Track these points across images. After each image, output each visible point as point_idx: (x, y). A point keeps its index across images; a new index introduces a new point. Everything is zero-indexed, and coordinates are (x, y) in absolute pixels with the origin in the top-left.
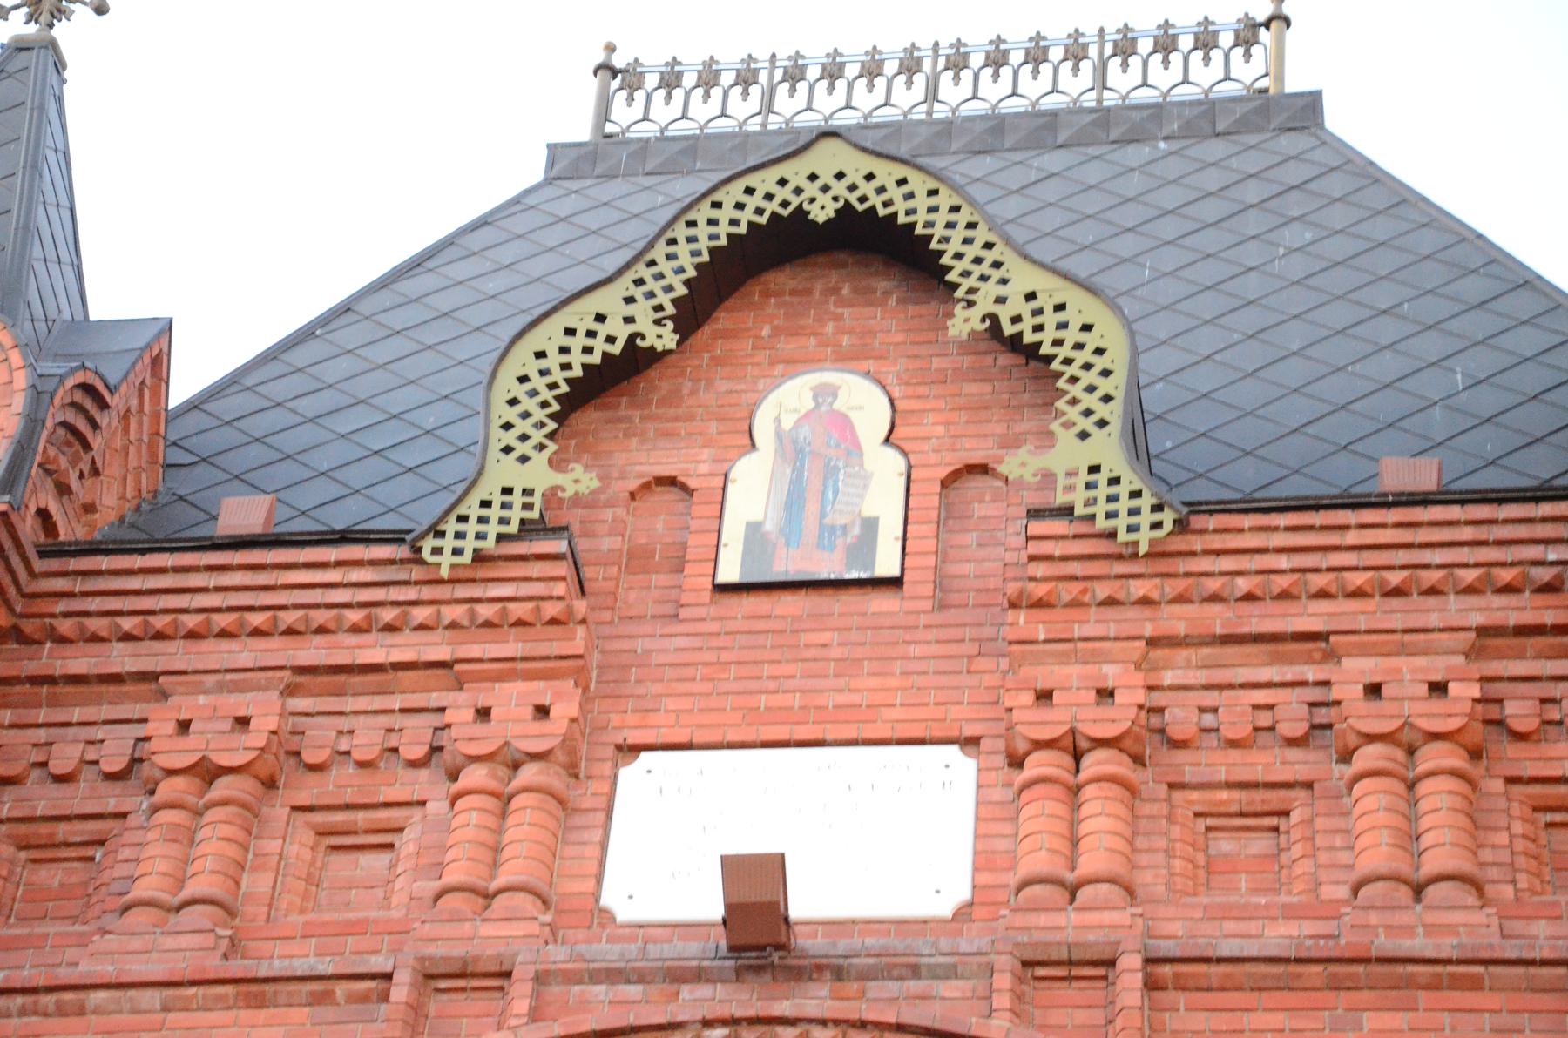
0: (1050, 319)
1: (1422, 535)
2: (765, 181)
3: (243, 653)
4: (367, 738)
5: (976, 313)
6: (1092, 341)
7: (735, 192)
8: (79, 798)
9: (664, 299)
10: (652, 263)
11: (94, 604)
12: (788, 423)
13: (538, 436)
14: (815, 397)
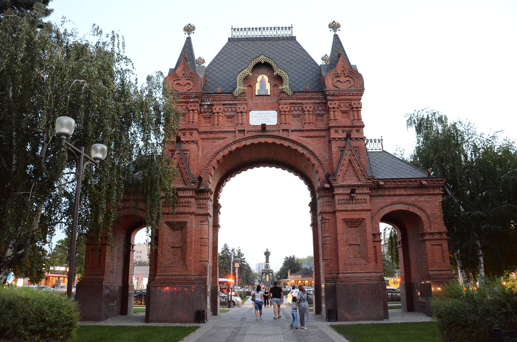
0: (282, 74)
2: (258, 59)
6: (285, 76)
7: (255, 60)
13: (242, 84)
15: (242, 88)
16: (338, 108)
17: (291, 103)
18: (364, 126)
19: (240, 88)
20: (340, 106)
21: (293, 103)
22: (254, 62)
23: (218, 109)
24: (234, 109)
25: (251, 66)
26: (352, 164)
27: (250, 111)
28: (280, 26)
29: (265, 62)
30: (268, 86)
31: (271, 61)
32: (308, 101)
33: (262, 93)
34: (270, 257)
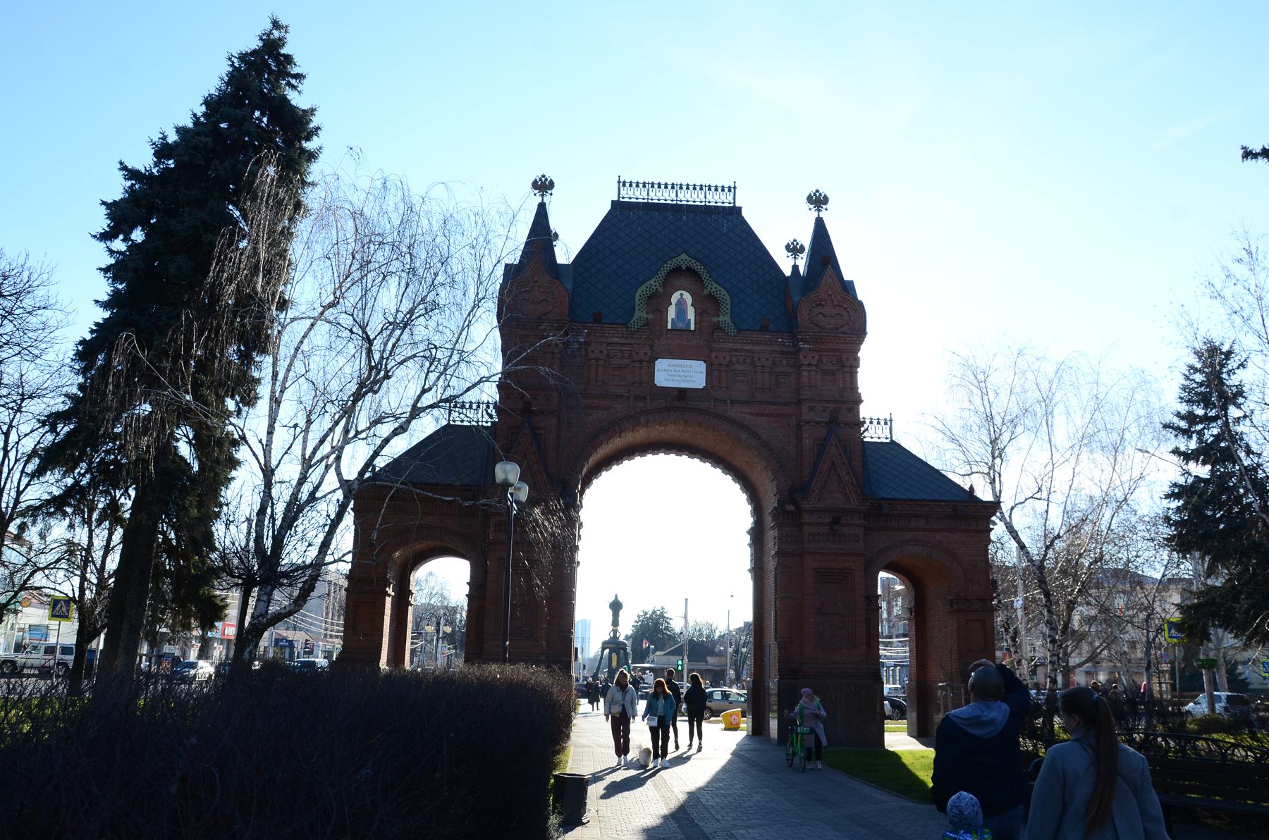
2: (675, 260)
15: (644, 315)
16: (817, 366)
17: (731, 350)
18: (862, 401)
19: (640, 314)
20: (820, 361)
21: (736, 350)
22: (669, 266)
23: (597, 351)
24: (627, 355)
25: (662, 274)
26: (836, 470)
27: (657, 359)
28: (713, 184)
29: (687, 267)
30: (691, 314)
31: (699, 267)
32: (762, 348)
33: (680, 325)
34: (621, 613)
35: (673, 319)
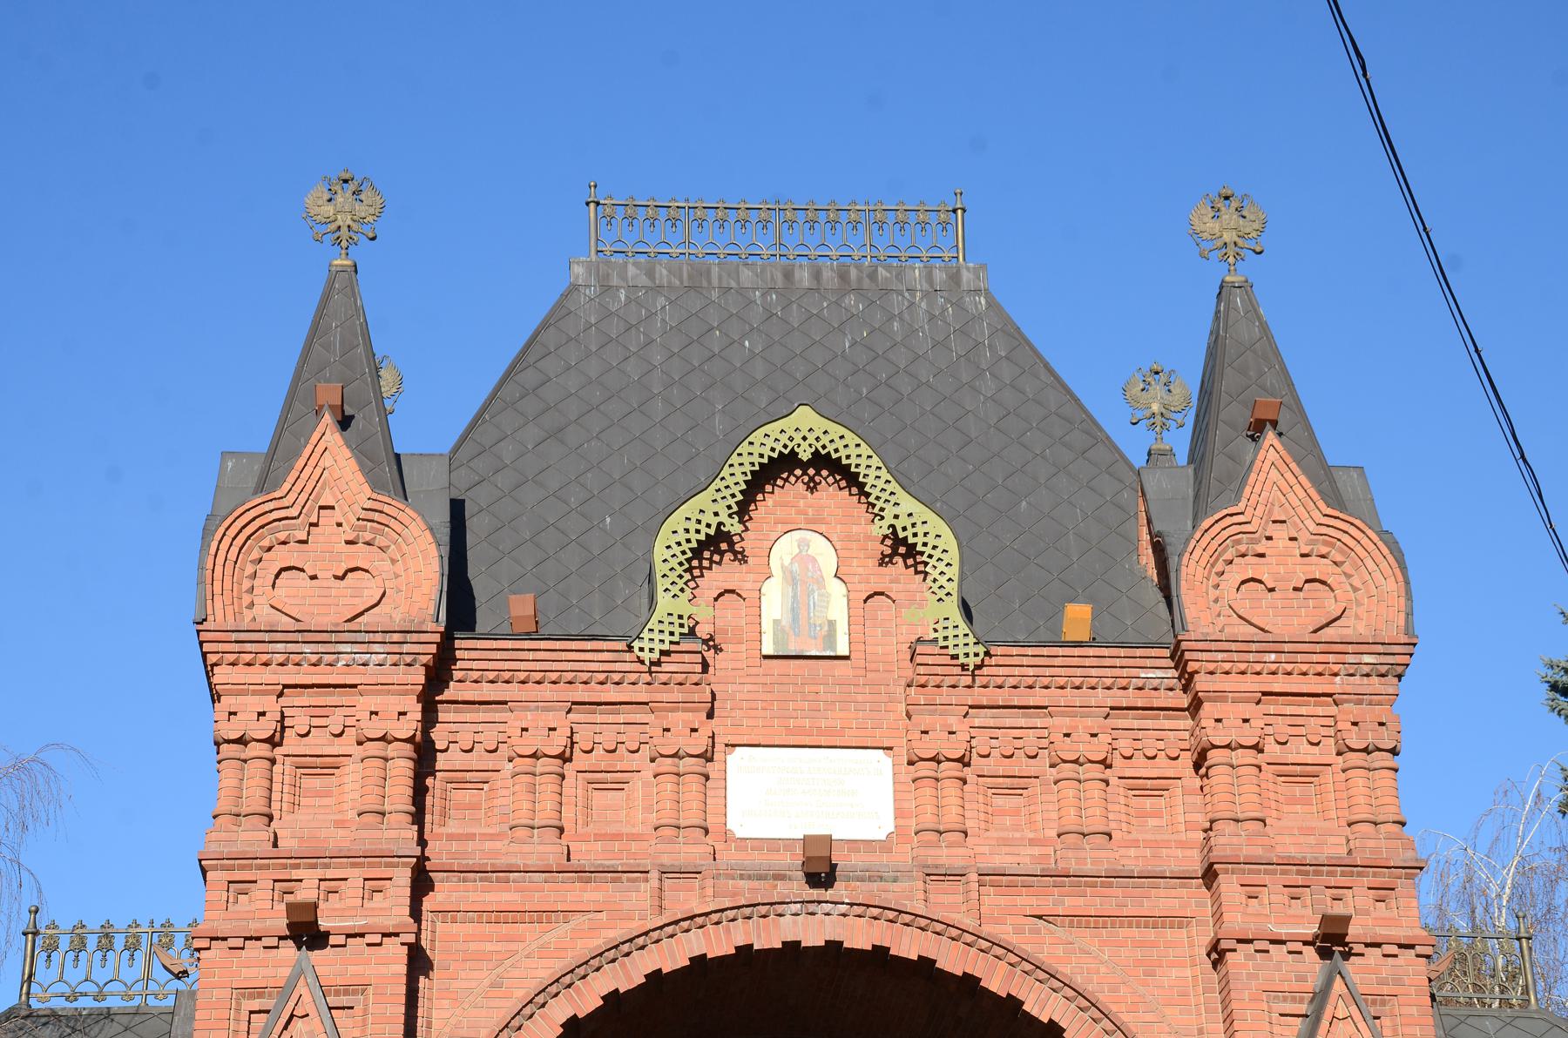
0: (920, 529)
1: (1087, 662)
3: (547, 691)
4: (608, 737)
5: (885, 523)
8: (473, 761)
9: (732, 502)
10: (723, 479)
11: (475, 665)
12: (787, 562)
14: (799, 547)
25: (736, 476)
29: (816, 453)
30: (836, 604)
35: (776, 622)
